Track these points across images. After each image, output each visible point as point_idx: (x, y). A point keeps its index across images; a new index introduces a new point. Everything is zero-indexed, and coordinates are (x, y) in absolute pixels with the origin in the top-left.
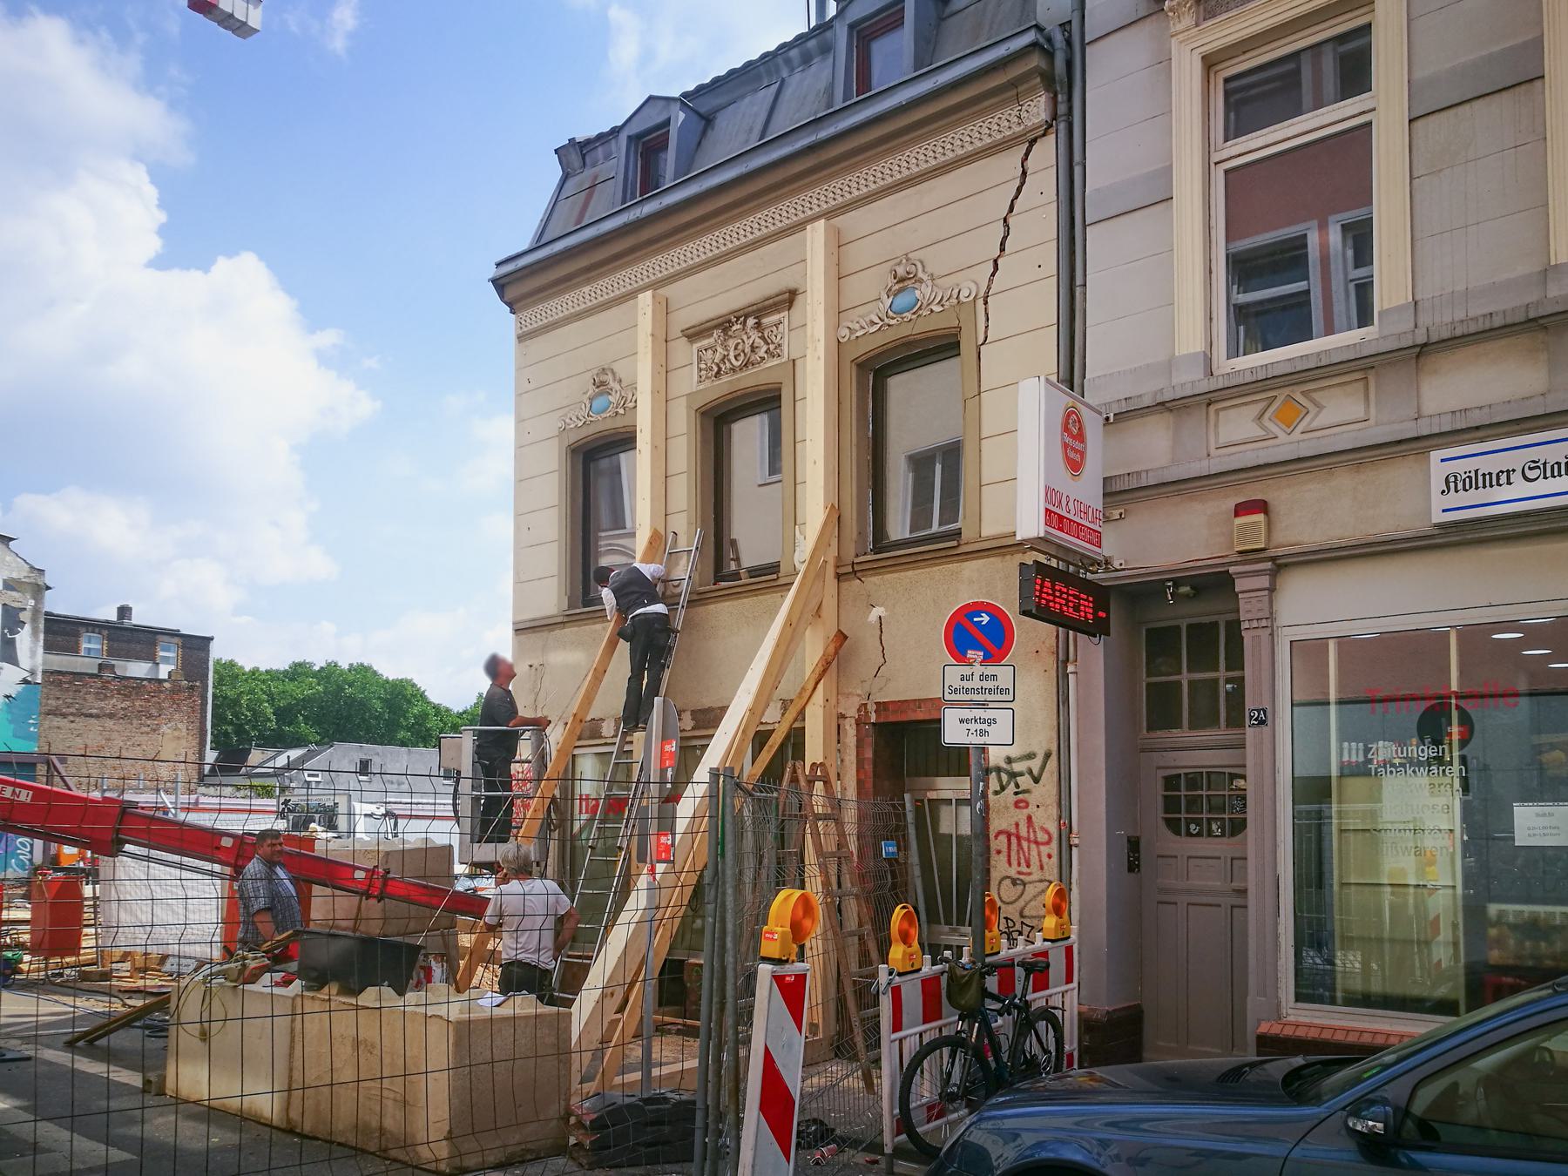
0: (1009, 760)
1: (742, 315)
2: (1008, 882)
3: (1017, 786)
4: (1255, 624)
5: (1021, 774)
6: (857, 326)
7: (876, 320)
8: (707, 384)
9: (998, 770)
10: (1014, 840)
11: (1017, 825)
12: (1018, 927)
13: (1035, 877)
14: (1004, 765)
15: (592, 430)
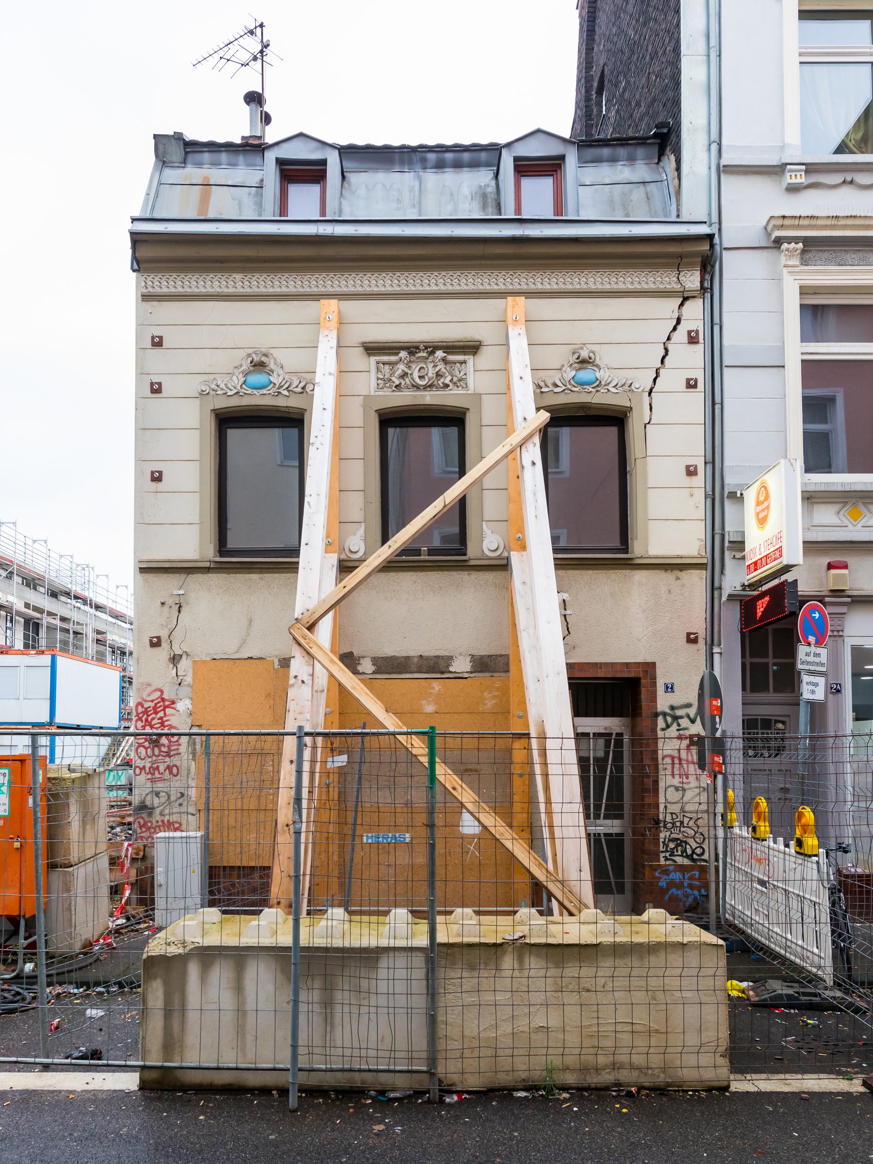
0: (672, 708)
1: (432, 348)
2: (672, 789)
3: (679, 725)
4: (836, 633)
5: (681, 717)
6: (542, 384)
7: (559, 384)
8: (387, 392)
9: (665, 714)
10: (676, 761)
11: (679, 750)
12: (680, 818)
13: (692, 785)
14: (668, 711)
15: (245, 401)
